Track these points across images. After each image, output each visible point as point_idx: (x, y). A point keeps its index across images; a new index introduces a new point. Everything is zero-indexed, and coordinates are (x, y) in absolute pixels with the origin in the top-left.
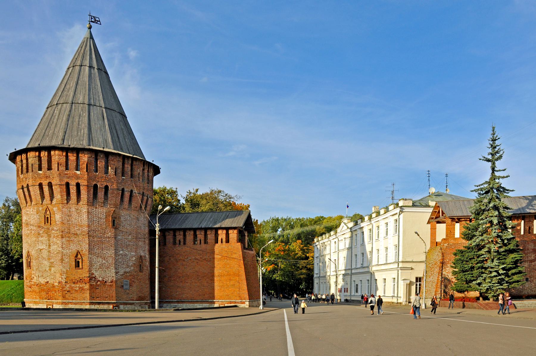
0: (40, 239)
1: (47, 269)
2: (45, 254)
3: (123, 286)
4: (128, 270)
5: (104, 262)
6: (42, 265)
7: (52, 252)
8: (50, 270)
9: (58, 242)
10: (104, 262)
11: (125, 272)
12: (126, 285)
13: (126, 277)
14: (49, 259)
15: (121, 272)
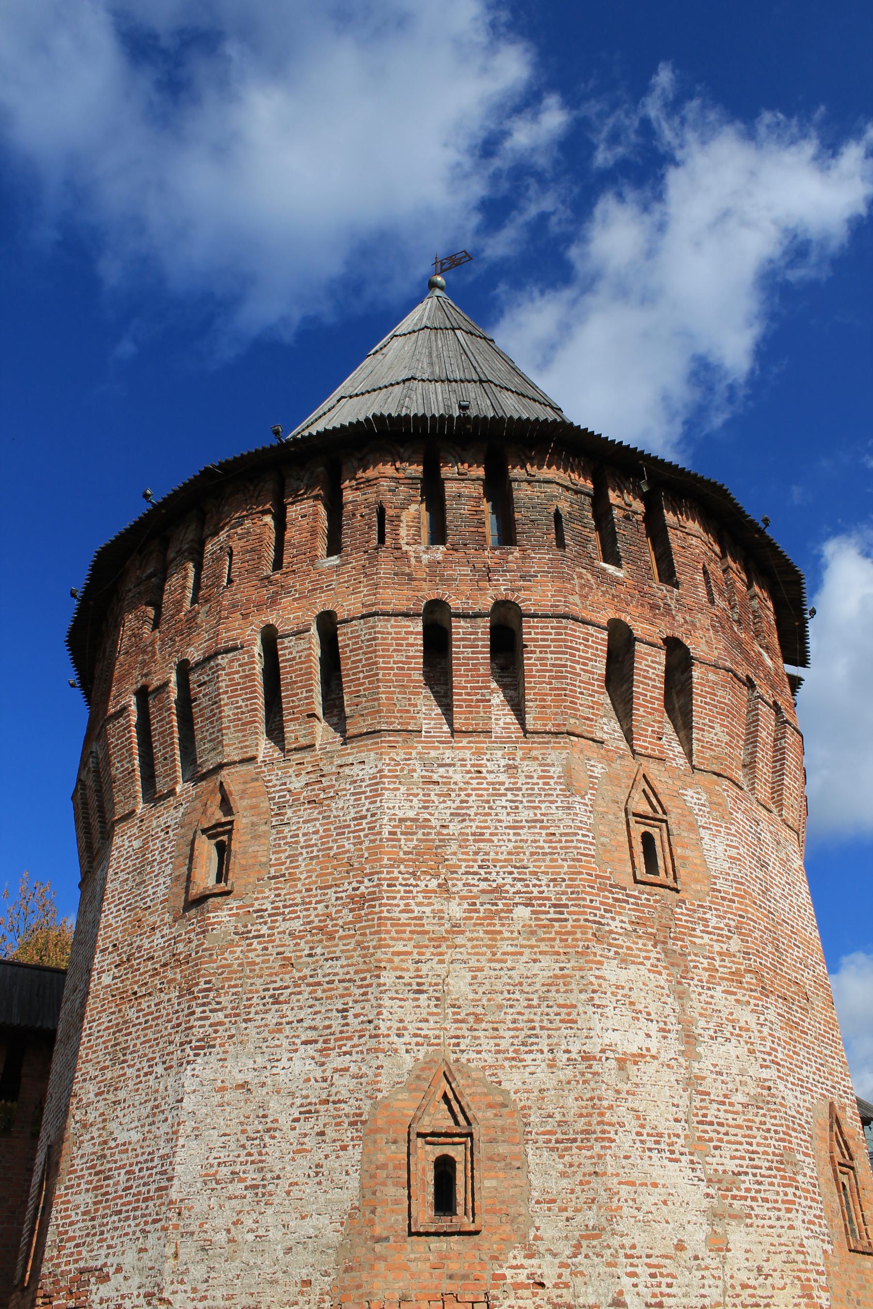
0: (612, 972)
1: (697, 1236)
2: (659, 1097)
6: (649, 1199)
7: (716, 1090)
8: (719, 1246)
9: (745, 1016)
14: (699, 1146)
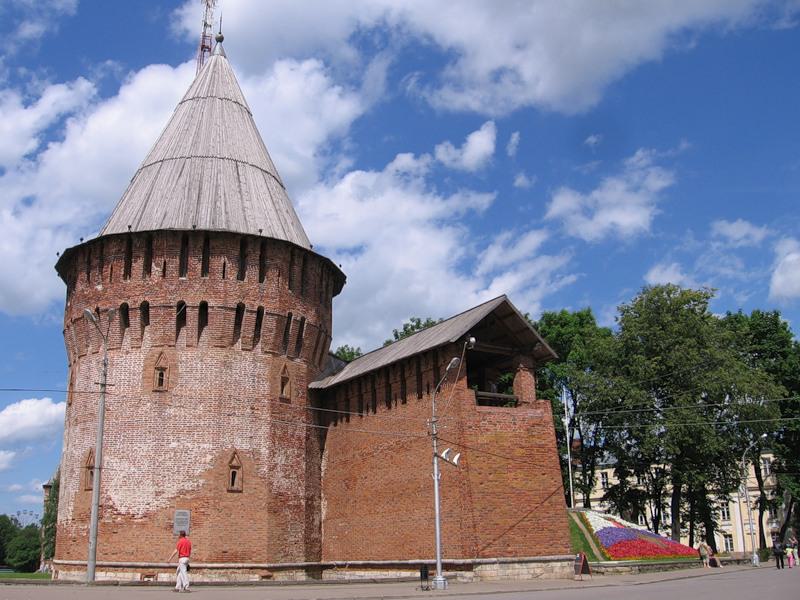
3: (172, 526)
4: (188, 486)
5: (133, 469)
10: (133, 469)
11: (181, 492)
12: (181, 523)
13: (184, 503)
15: (171, 489)
